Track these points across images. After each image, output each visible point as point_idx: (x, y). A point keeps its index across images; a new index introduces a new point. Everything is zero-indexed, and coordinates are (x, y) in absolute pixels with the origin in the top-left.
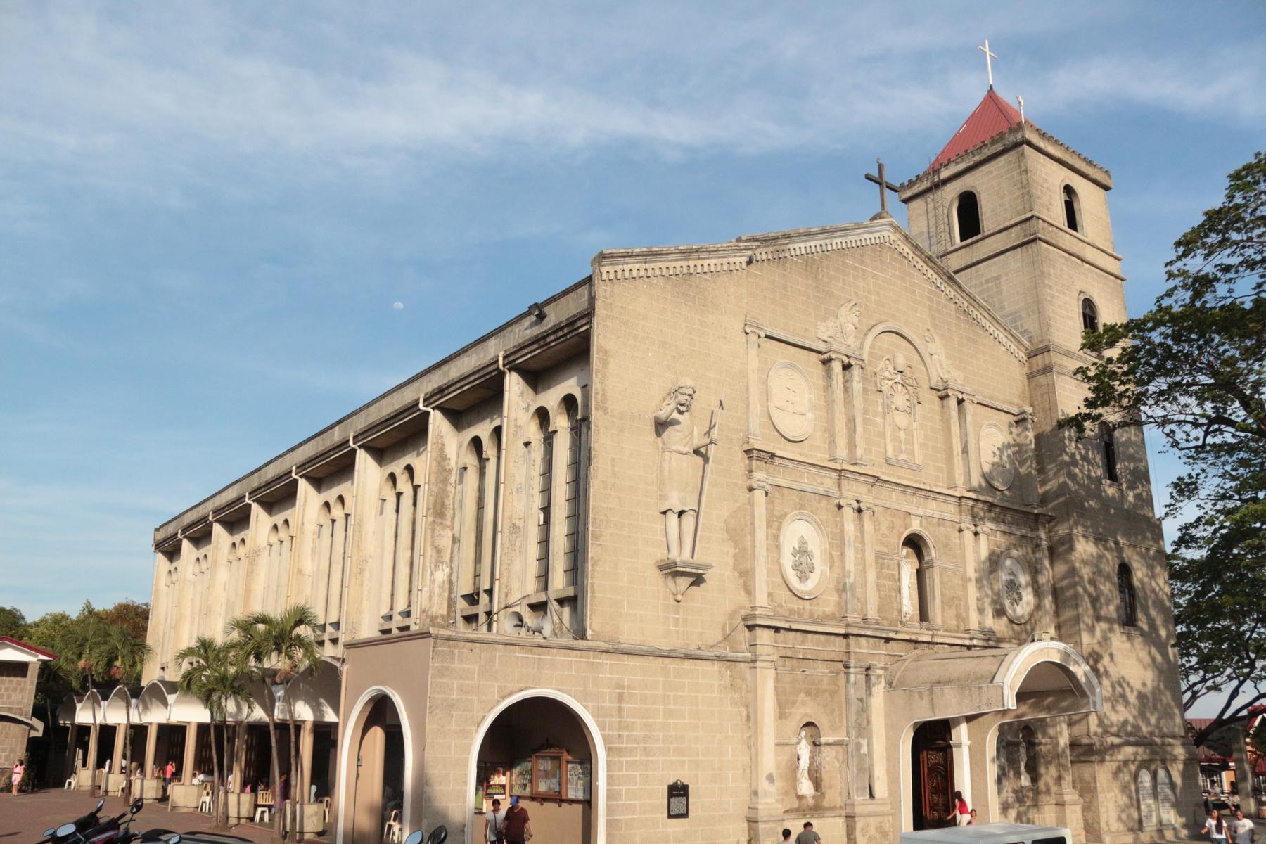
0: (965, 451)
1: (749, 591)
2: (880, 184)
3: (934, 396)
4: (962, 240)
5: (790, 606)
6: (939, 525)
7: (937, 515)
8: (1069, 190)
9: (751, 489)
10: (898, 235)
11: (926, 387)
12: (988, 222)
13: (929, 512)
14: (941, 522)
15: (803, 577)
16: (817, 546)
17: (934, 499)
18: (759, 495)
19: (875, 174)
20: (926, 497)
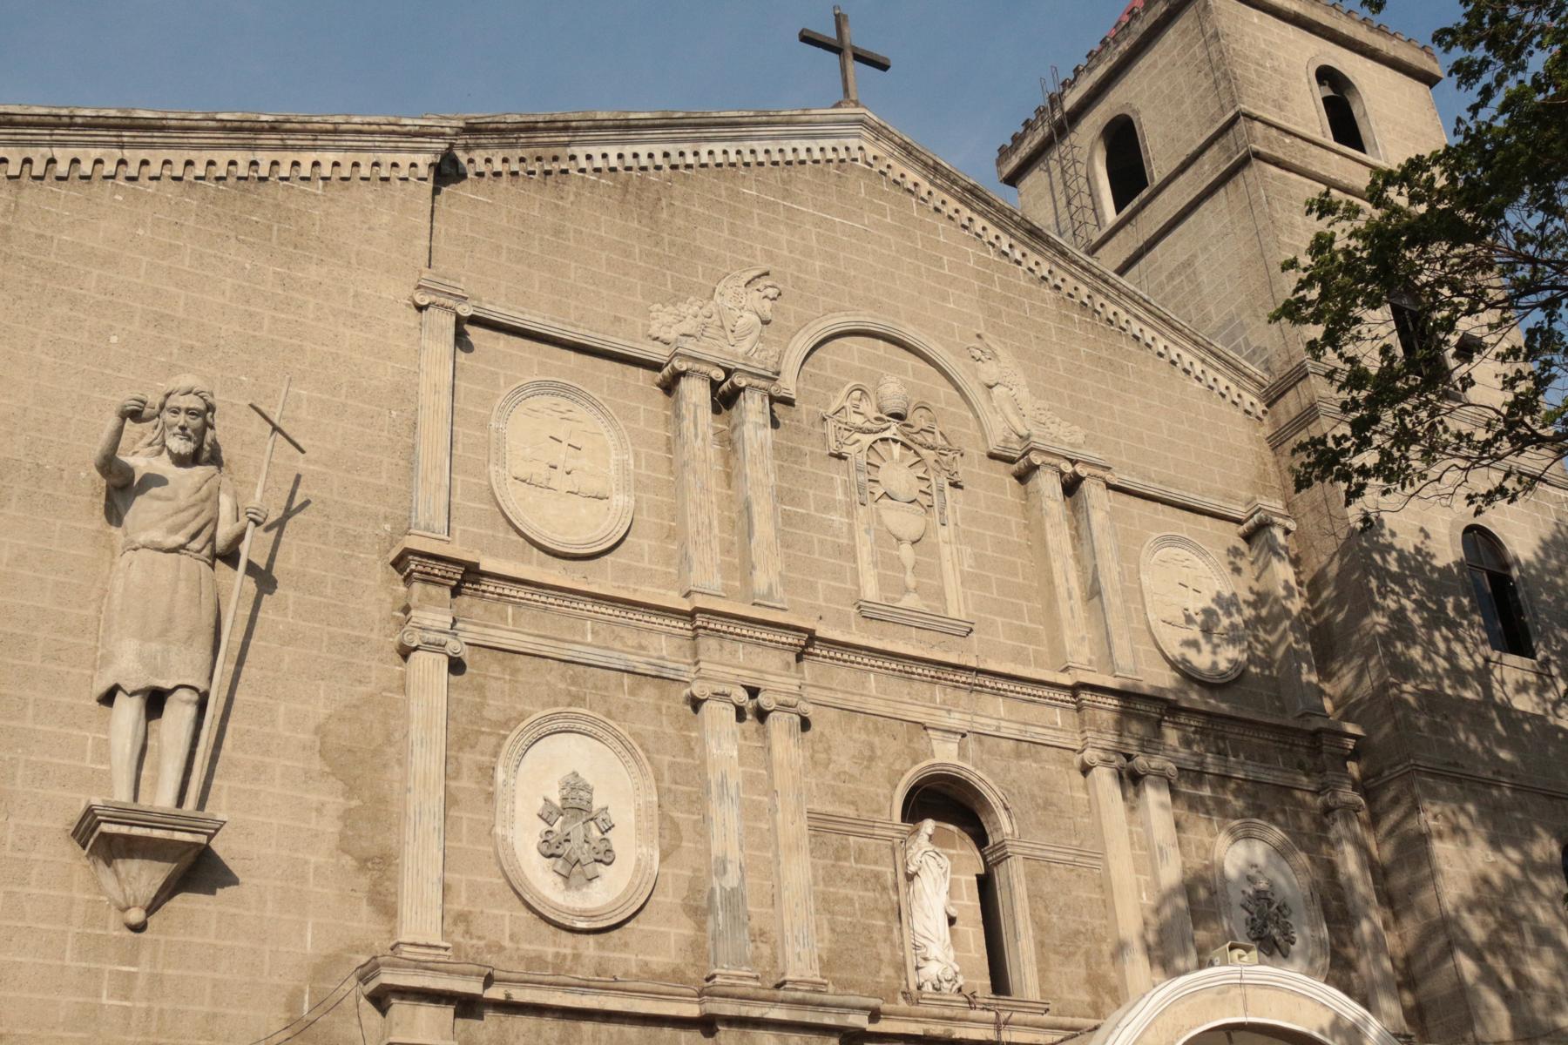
0: (1094, 592)
1: (387, 909)
2: (836, 49)
3: (1003, 475)
4: (1118, 211)
5: (529, 948)
6: (1019, 755)
7: (1010, 730)
8: (1326, 75)
9: (405, 653)
10: (884, 144)
11: (976, 453)
12: (1159, 161)
13: (986, 724)
14: (1026, 746)
15: (573, 871)
16: (621, 792)
17: (997, 692)
18: (429, 669)
19: (830, 33)
20: (973, 689)
